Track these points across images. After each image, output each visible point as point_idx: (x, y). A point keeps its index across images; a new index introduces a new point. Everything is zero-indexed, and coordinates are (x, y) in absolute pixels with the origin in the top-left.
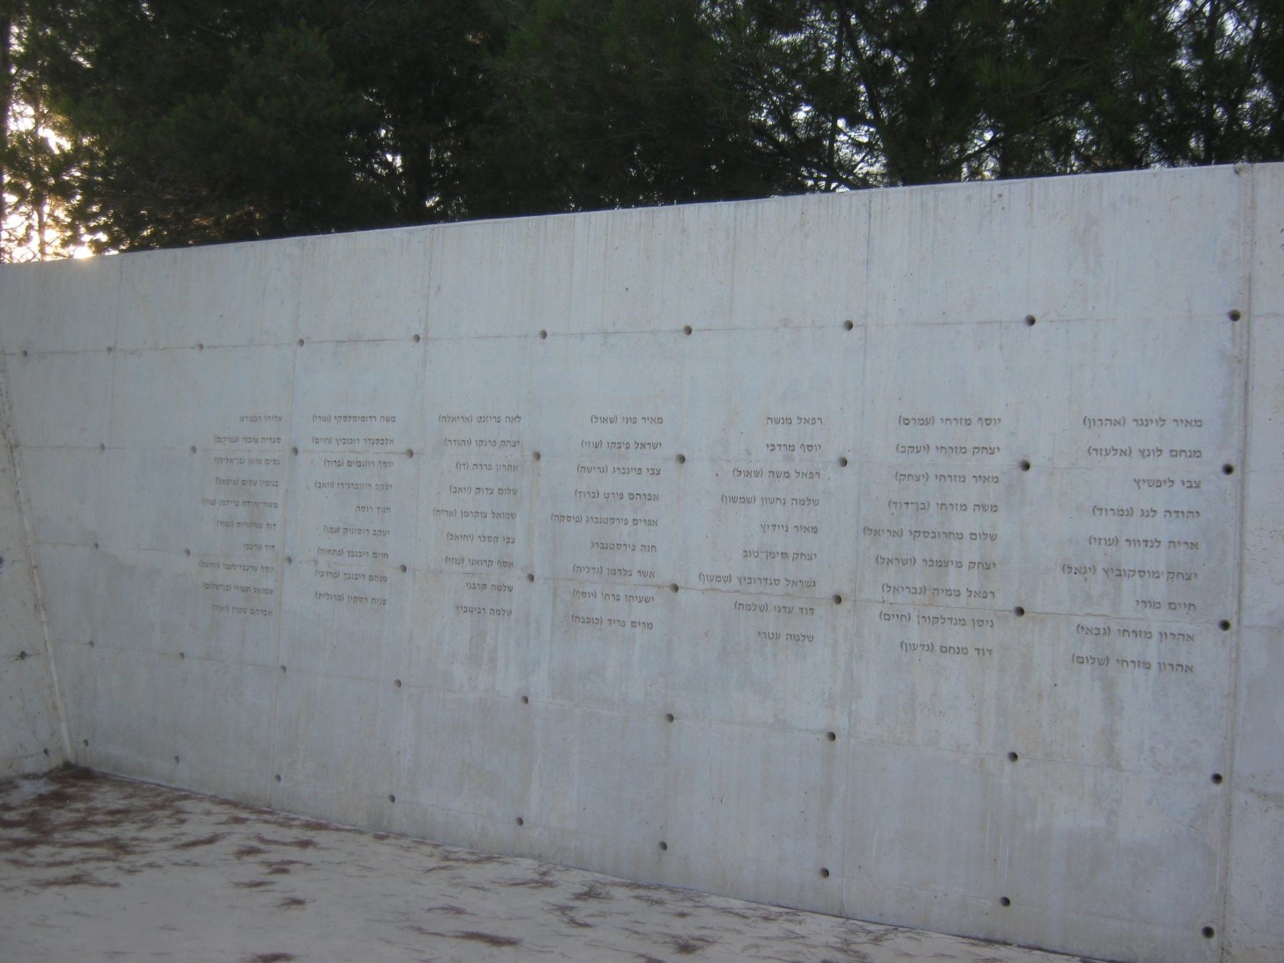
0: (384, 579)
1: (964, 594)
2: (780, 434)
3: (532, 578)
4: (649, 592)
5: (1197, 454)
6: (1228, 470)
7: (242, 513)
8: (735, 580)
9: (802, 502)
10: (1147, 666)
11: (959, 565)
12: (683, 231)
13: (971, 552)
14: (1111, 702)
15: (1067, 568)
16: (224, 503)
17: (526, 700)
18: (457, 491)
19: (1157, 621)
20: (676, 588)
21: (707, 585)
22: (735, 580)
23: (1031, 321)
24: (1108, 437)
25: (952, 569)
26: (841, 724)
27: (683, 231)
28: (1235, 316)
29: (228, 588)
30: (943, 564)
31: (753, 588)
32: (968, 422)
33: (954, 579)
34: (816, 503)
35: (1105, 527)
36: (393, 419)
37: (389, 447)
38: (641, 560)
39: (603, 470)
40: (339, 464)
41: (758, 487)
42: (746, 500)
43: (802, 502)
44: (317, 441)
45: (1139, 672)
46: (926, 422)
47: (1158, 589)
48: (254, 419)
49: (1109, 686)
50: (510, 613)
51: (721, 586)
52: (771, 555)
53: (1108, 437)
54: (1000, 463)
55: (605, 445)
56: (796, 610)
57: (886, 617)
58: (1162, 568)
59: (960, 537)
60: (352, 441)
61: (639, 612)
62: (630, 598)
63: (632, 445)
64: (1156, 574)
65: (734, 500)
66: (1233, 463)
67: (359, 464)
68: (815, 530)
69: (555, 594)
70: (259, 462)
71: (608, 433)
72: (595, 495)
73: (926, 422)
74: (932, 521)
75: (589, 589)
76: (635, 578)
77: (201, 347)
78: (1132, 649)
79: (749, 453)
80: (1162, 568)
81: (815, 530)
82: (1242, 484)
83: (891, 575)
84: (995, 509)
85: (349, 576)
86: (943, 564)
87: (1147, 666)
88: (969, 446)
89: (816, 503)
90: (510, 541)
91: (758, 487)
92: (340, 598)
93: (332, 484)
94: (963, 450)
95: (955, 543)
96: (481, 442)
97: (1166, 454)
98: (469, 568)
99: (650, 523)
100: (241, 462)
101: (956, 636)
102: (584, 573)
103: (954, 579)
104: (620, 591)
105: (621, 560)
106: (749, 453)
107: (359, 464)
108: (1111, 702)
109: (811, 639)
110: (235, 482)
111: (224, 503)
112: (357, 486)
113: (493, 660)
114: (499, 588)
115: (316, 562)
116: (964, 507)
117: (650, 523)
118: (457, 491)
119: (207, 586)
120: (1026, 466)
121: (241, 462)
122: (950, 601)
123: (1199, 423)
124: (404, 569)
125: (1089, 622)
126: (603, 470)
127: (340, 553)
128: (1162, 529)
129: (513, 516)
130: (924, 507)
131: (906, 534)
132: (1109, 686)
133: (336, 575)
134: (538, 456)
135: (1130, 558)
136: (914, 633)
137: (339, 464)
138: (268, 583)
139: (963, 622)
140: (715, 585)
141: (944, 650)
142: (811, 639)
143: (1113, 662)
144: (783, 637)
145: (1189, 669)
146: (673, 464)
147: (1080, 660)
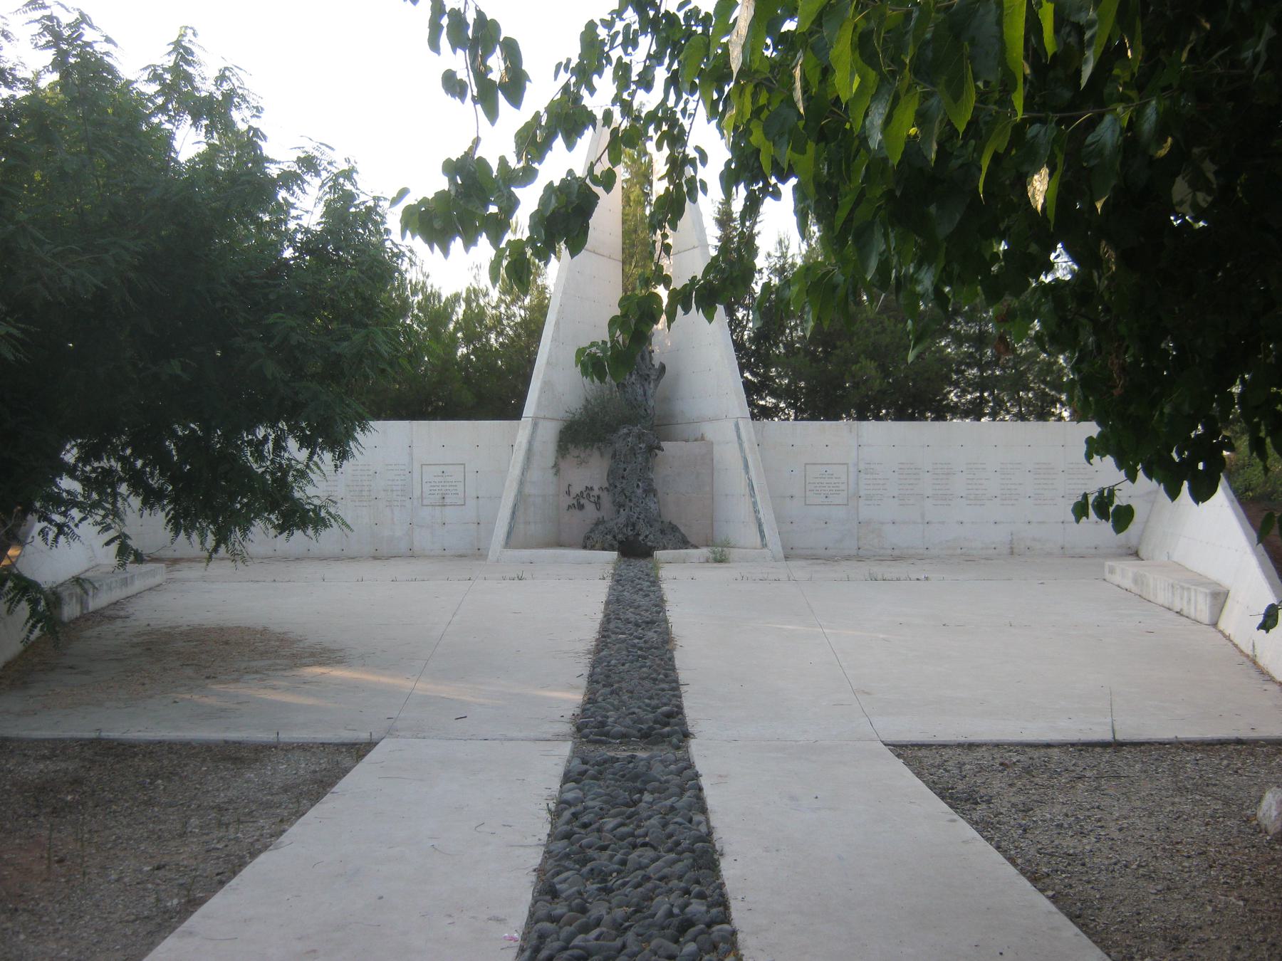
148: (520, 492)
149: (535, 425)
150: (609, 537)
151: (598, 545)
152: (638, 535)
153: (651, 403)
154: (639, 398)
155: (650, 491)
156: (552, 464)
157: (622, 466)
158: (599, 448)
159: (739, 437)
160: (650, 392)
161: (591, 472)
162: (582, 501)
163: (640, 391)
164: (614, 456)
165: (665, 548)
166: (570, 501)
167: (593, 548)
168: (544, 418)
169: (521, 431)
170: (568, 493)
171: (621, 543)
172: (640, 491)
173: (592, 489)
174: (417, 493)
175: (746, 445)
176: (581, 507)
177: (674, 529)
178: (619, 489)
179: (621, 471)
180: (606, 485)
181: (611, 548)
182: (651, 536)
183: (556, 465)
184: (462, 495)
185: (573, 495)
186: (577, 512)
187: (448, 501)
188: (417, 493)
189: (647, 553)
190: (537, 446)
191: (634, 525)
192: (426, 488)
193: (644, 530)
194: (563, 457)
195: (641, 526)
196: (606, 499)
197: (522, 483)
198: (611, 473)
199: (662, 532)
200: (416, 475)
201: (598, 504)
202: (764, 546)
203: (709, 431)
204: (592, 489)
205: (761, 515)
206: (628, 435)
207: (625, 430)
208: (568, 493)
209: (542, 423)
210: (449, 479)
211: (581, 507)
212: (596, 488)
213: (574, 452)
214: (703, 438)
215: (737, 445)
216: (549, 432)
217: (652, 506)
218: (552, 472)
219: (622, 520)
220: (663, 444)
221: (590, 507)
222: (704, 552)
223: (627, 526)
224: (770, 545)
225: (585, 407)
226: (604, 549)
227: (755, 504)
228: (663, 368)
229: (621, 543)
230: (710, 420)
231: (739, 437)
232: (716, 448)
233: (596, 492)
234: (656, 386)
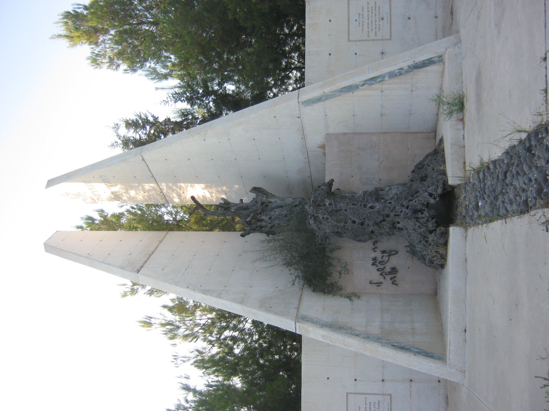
148: (378, 339)
149: (304, 319)
150: (431, 237)
151: (441, 251)
152: (428, 205)
153: (289, 201)
154: (284, 212)
155: (377, 195)
156: (346, 302)
157: (349, 225)
158: (331, 251)
159: (319, 100)
160: (279, 202)
161: (357, 260)
162: (388, 269)
163: (278, 211)
164: (339, 234)
165: (444, 173)
166: (387, 282)
167: (444, 257)
168: (298, 308)
169: (310, 333)
170: (379, 284)
171: (438, 225)
172: (378, 206)
173: (374, 259)
175: (327, 90)
176: (394, 270)
177: (420, 167)
178: (375, 228)
179: (355, 226)
180: (370, 244)
181: (445, 235)
182: (430, 190)
183: (349, 297)
184: (379, 398)
185: (381, 279)
186: (399, 275)
189: (449, 195)
190: (326, 318)
191: (416, 211)
193: (424, 197)
194: (340, 289)
195: (416, 203)
196: (387, 244)
197: (368, 337)
198: (358, 237)
199: (423, 179)
201: (391, 253)
202: (440, 59)
203: (315, 139)
204: (374, 259)
205: (405, 65)
206: (315, 218)
207: (312, 221)
208: (379, 284)
209: (302, 312)
211: (394, 270)
212: (373, 255)
213: (335, 277)
214: (323, 147)
215: (328, 102)
216: (315, 304)
217: (394, 191)
218: (356, 301)
219: (410, 224)
220: (327, 180)
221: (394, 261)
222: (448, 130)
223: (417, 219)
224: (441, 51)
225: (288, 264)
226: (446, 244)
227: (392, 75)
228: (256, 190)
229: (438, 225)
230: (304, 138)
231: (319, 100)
232: (331, 130)
233: (378, 255)
234: (273, 196)
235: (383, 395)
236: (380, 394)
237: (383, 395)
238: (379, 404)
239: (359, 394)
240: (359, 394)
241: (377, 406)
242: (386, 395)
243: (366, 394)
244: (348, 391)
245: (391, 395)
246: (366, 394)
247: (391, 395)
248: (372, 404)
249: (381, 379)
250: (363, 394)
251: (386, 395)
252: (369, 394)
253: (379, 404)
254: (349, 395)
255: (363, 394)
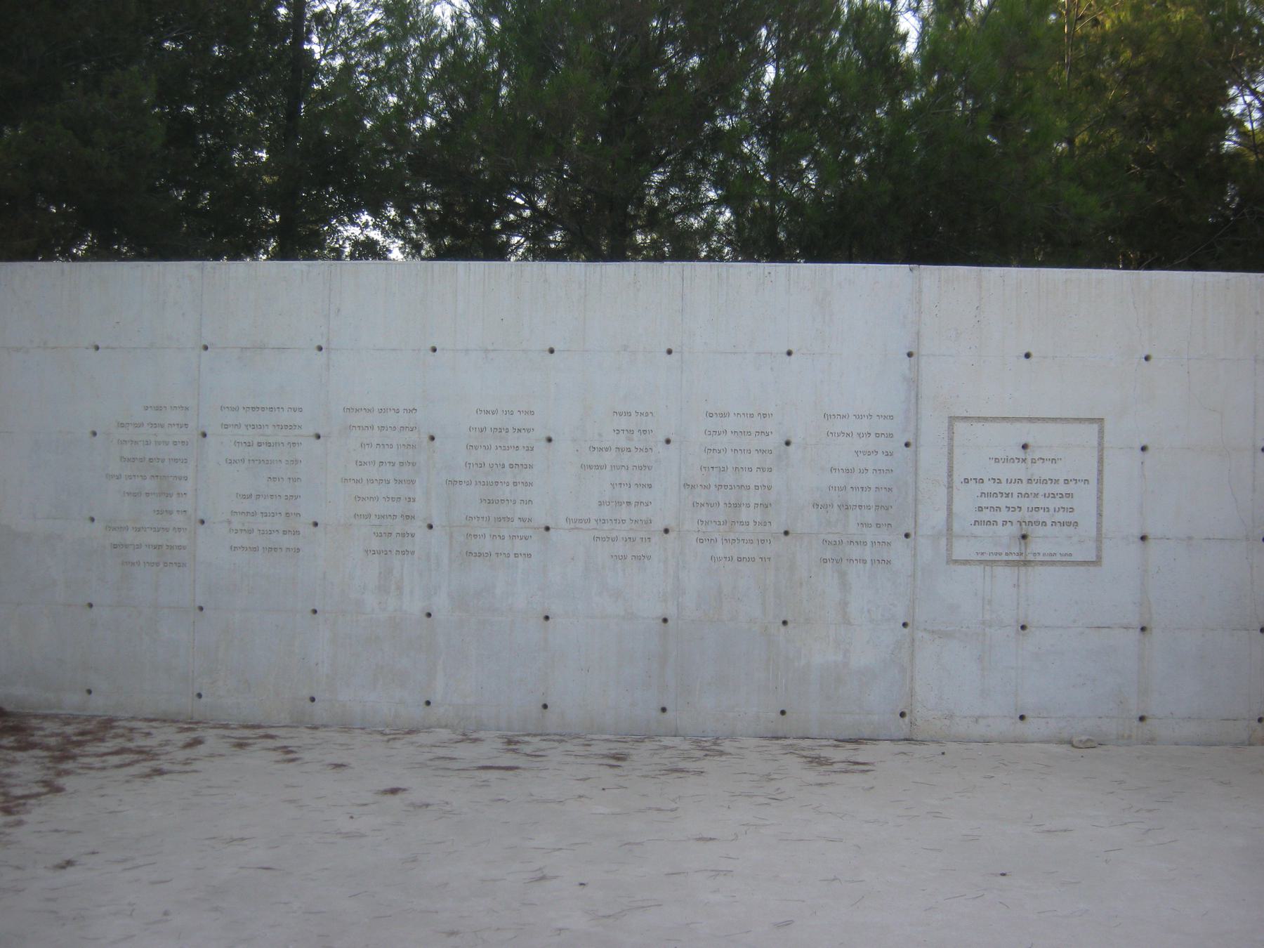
0: (297, 532)
1: (752, 524)
2: (623, 423)
3: (431, 527)
4: (528, 533)
5: (891, 435)
6: (907, 445)
7: (150, 485)
8: (593, 522)
9: (641, 468)
10: (864, 562)
11: (748, 506)
12: (546, 281)
13: (756, 498)
14: (844, 585)
15: (816, 505)
16: (130, 477)
17: (429, 615)
18: (362, 464)
19: (870, 535)
20: (547, 529)
21: (572, 525)
22: (593, 522)
23: (789, 353)
24: (839, 426)
25: (743, 508)
26: (671, 612)
27: (546, 281)
28: (910, 355)
29: (139, 546)
30: (737, 505)
31: (606, 526)
32: (752, 416)
33: (745, 515)
34: (650, 468)
35: (838, 480)
36: (301, 410)
37: (297, 432)
38: (521, 511)
39: (487, 448)
40: (249, 445)
41: (608, 458)
42: (598, 467)
43: (641, 468)
44: (226, 426)
45: (861, 565)
46: (723, 415)
47: (870, 516)
48: (158, 408)
49: (843, 575)
50: (413, 553)
51: (583, 525)
52: (620, 503)
53: (839, 426)
54: (774, 441)
55: (488, 430)
56: (638, 540)
57: (701, 541)
58: (872, 504)
59: (748, 488)
60: (261, 427)
61: (520, 546)
62: (513, 537)
63: (511, 430)
64: (869, 508)
65: (590, 467)
66: (911, 441)
67: (269, 444)
68: (650, 486)
69: (451, 537)
70: (167, 443)
71: (490, 421)
72: (482, 465)
73: (723, 415)
74: (729, 478)
75: (479, 532)
76: (517, 523)
77: (97, 348)
78: (855, 552)
79: (600, 435)
80: (872, 504)
81: (650, 486)
82: (916, 453)
83: (703, 514)
84: (770, 470)
85: (262, 532)
86: (737, 505)
87: (864, 562)
88: (753, 431)
89: (650, 468)
90: (411, 500)
91: (608, 458)
92: (255, 549)
93: (243, 461)
94: (749, 433)
95: (745, 492)
96: (382, 428)
97: (873, 435)
98: (377, 522)
99: (526, 484)
100: (148, 443)
101: (747, 550)
102: (475, 521)
103: (745, 515)
104: (505, 532)
105: (504, 510)
106: (600, 435)
107: (269, 444)
108: (844, 585)
109: (649, 558)
110: (142, 460)
111: (130, 477)
112: (267, 462)
113: (399, 588)
114: (403, 535)
115: (229, 522)
116: (750, 469)
117: (526, 484)
118: (362, 464)
119: (115, 546)
120: (788, 443)
121: (148, 443)
122: (743, 528)
123: (891, 417)
124: (316, 524)
125: (830, 538)
126: (487, 448)
127: (254, 514)
128: (871, 480)
129: (413, 482)
130: (724, 469)
131: (713, 487)
132: (843, 575)
133: (250, 531)
134: (432, 438)
135: (853, 498)
136: (720, 550)
137: (249, 445)
138: (181, 540)
139: (751, 542)
140: (579, 525)
141: (740, 559)
142: (649, 558)
143: (845, 561)
144: (629, 557)
145: (889, 562)
146: (544, 443)
147: (825, 561)
174: (933, 517)
187: (1039, 547)
188: (933, 517)
192: (965, 501)
200: (931, 457)
210: (1044, 471)
235: (1099, 539)
236: (1099, 529)
237: (1099, 539)
238: (1069, 524)
239: (1101, 461)
240: (1101, 461)
241: (1061, 516)
242: (1099, 549)
243: (1100, 480)
244: (1108, 426)
245: (1097, 562)
246: (1100, 480)
247: (1097, 562)
248: (1065, 503)
249: (1149, 531)
250: (1100, 472)
251: (1099, 549)
252: (1100, 492)
253: (1069, 524)
254: (1095, 426)
255: (1100, 472)
